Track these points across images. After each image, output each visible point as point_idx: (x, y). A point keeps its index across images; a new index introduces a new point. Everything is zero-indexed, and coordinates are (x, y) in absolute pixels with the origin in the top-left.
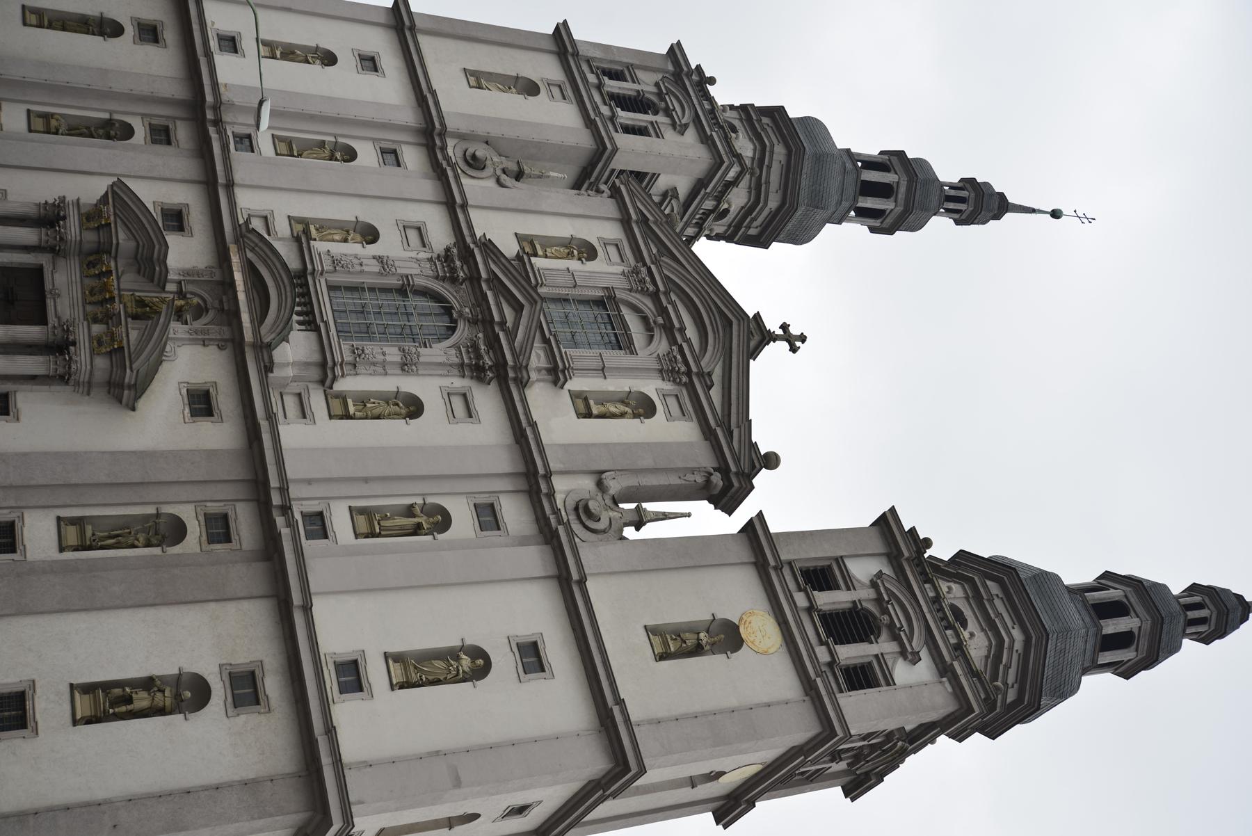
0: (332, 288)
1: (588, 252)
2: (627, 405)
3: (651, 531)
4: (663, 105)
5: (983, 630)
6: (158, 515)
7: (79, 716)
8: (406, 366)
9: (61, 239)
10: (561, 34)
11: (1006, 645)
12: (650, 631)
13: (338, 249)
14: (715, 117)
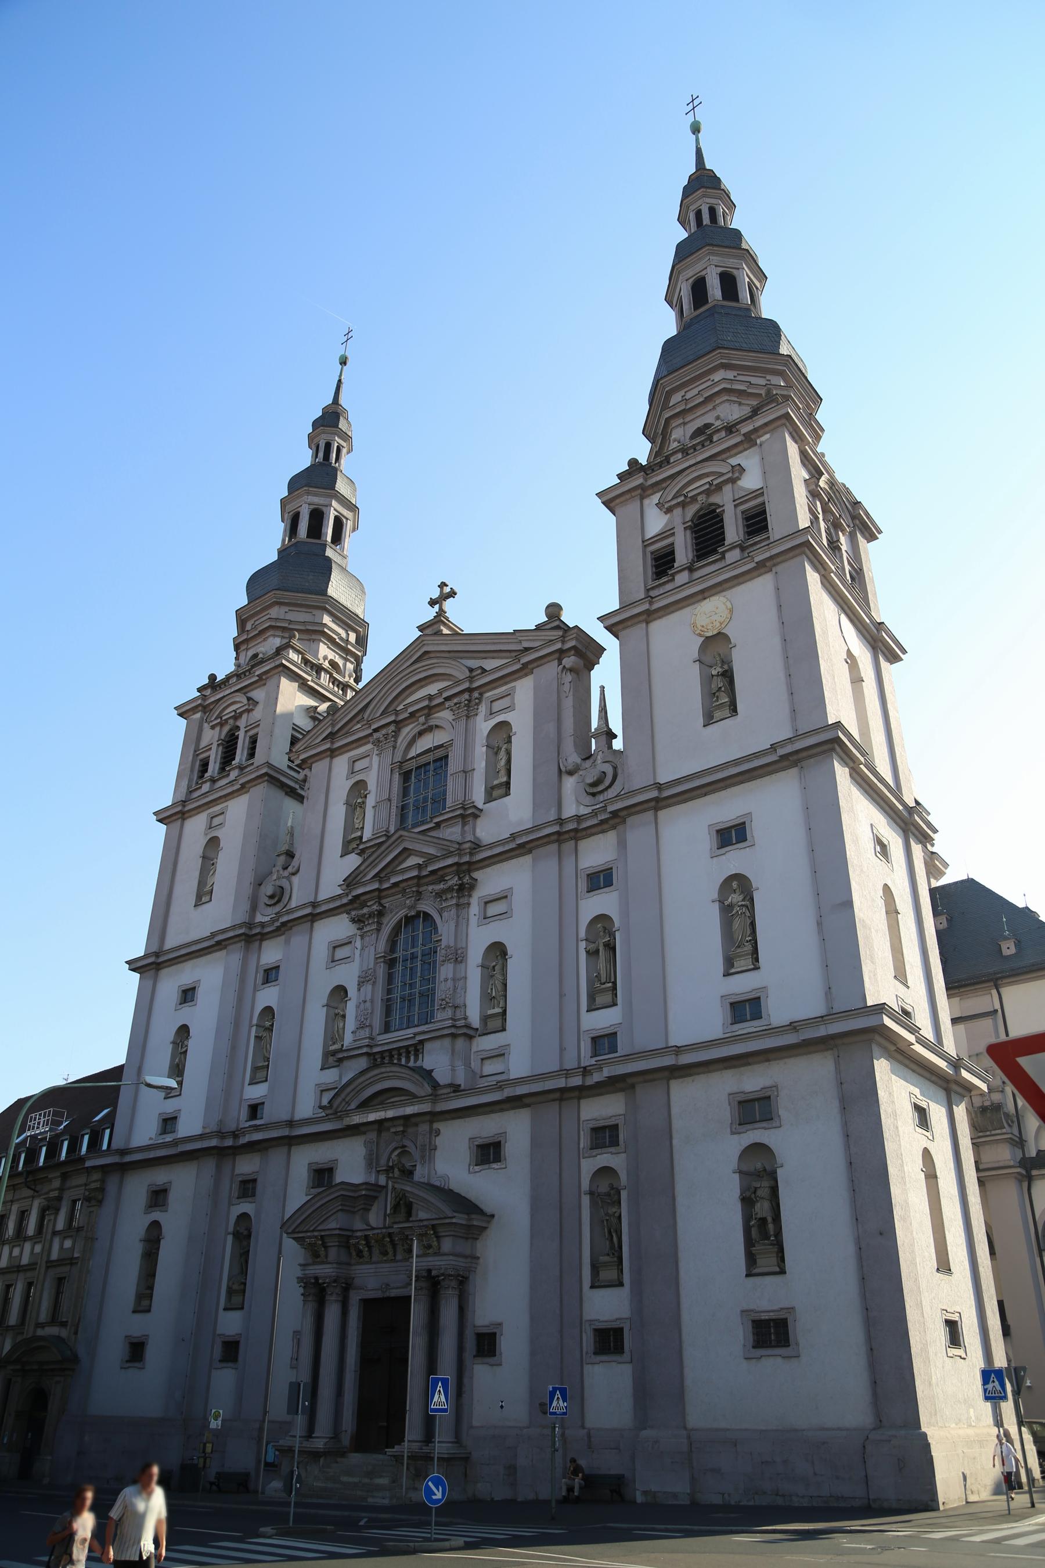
0: (387, 1028)
1: (359, 788)
2: (499, 749)
3: (616, 724)
4: (231, 722)
5: (714, 408)
6: (591, 1193)
7: (777, 1269)
8: (458, 957)
9: (335, 1281)
10: (164, 817)
11: (729, 386)
12: (709, 719)
13: (351, 1024)
14: (244, 673)
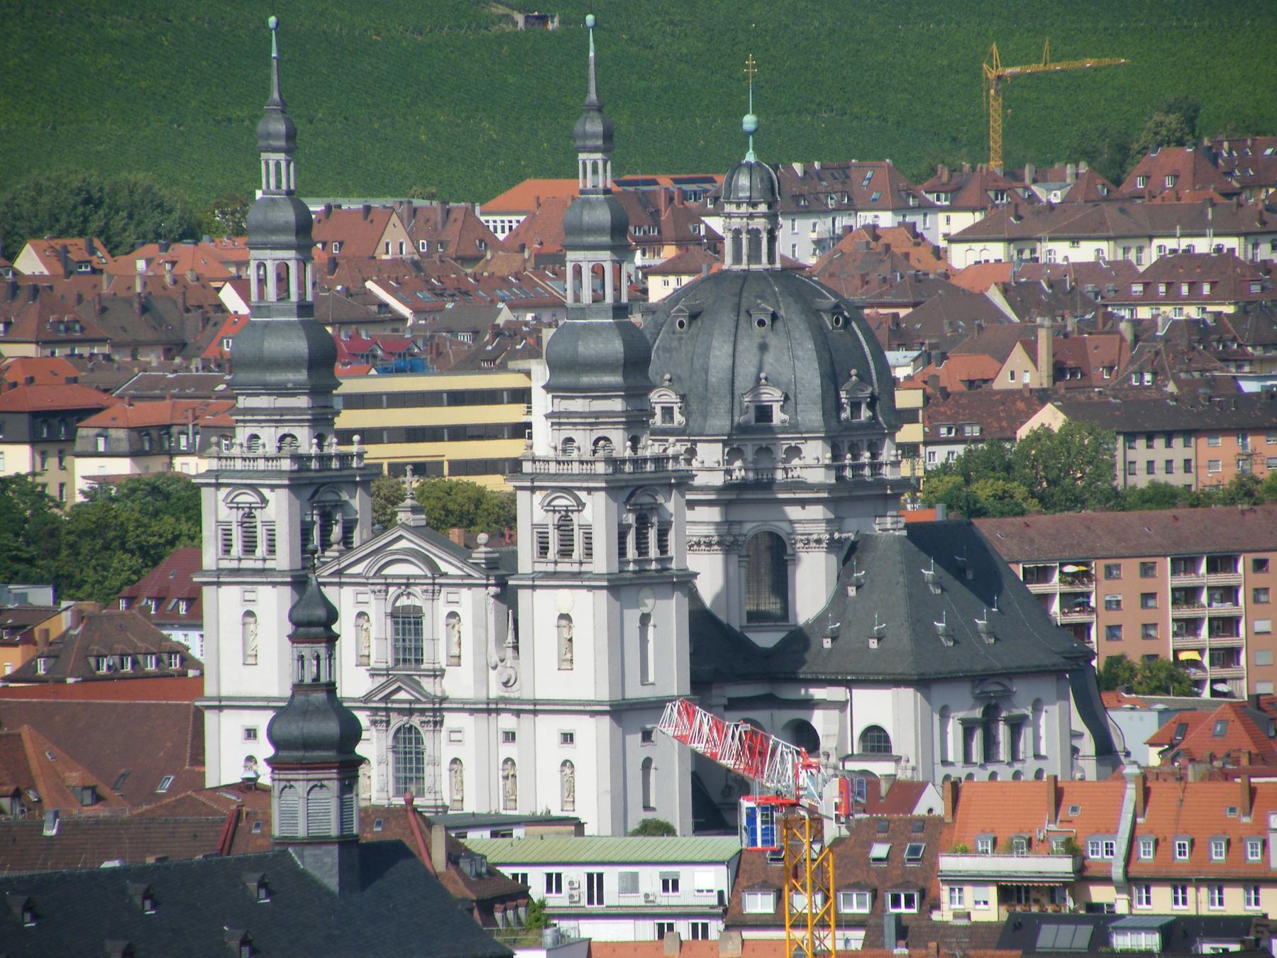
8: (435, 763)
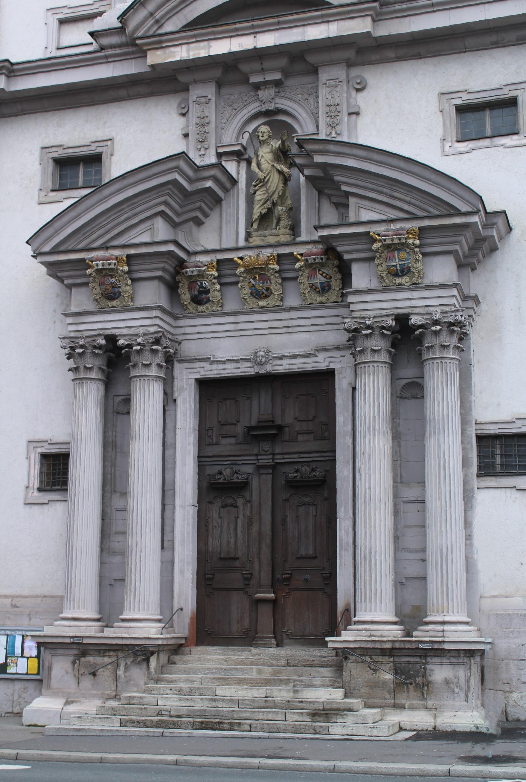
9: (157, 342)
